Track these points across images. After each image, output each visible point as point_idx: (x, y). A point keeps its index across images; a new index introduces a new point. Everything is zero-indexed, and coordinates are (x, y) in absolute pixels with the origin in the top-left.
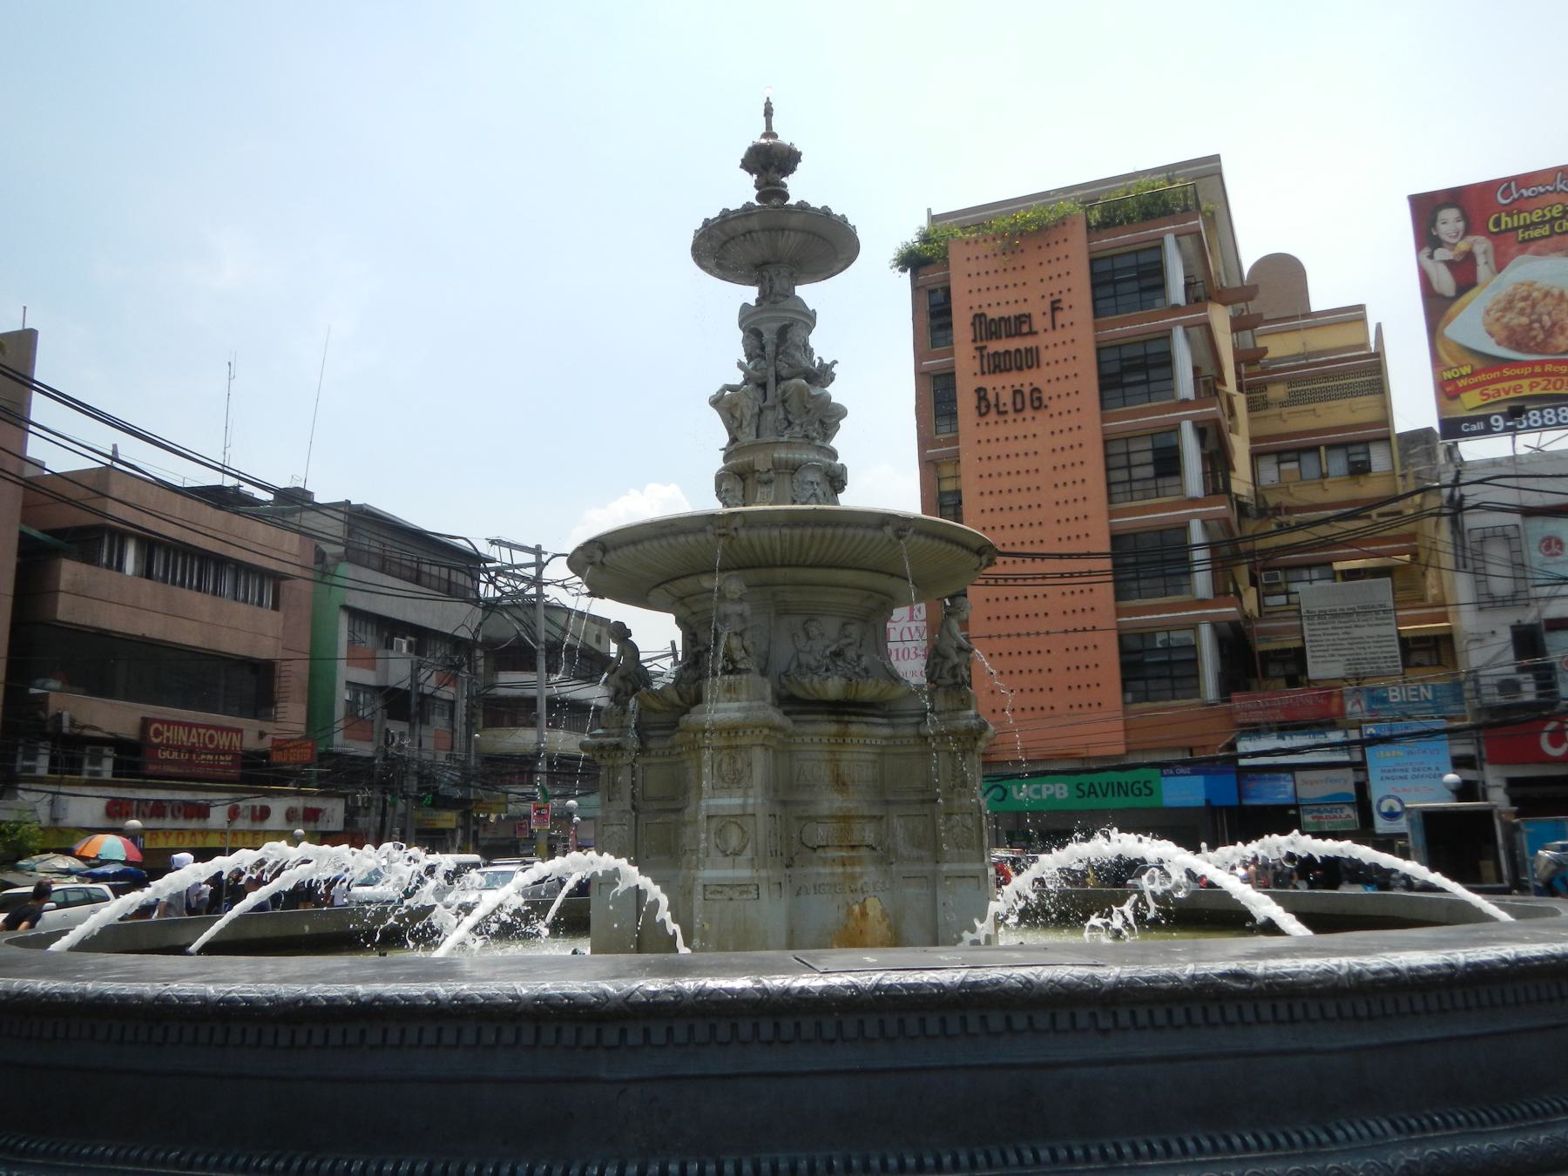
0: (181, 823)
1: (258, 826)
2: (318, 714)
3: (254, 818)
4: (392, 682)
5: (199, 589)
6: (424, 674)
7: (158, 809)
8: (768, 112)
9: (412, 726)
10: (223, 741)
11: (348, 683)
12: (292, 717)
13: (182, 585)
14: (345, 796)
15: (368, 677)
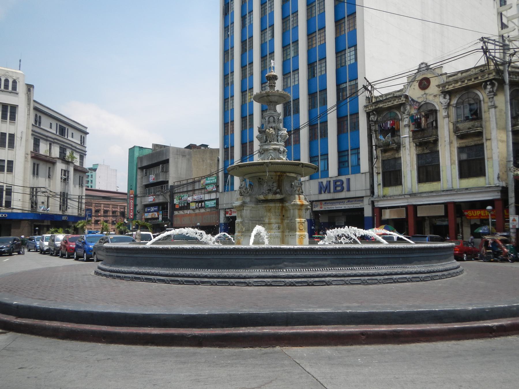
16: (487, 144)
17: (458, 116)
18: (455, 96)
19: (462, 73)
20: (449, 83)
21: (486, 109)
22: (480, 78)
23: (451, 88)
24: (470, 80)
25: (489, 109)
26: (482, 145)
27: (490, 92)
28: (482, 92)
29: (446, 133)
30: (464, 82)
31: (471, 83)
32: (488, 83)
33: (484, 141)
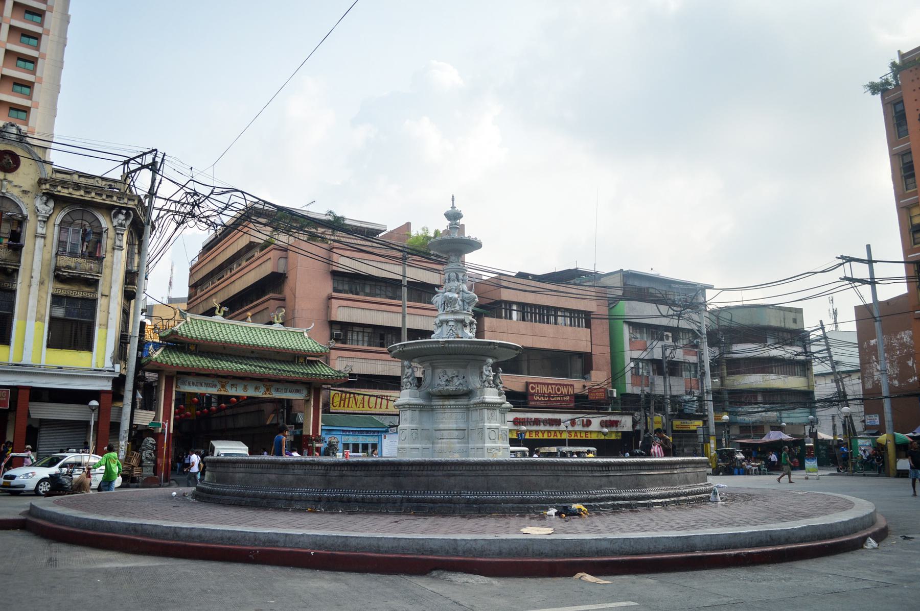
0: (548, 428)
1: (586, 429)
2: (616, 376)
3: (584, 426)
4: (656, 357)
5: (548, 323)
6: (668, 351)
7: (537, 422)
8: (453, 200)
9: (665, 378)
10: (564, 391)
11: (632, 359)
12: (599, 377)
13: (540, 322)
14: (632, 414)
15: (644, 355)
16: (101, 303)
17: (61, 243)
18: (63, 209)
19: (80, 176)
20: (64, 184)
21: (109, 248)
22: (115, 198)
23: (64, 192)
24: (101, 195)
25: (114, 249)
26: (94, 301)
27: (121, 225)
28: (108, 219)
29: (37, 266)
30: (89, 193)
31: (98, 200)
32: (124, 212)
33: (99, 295)
